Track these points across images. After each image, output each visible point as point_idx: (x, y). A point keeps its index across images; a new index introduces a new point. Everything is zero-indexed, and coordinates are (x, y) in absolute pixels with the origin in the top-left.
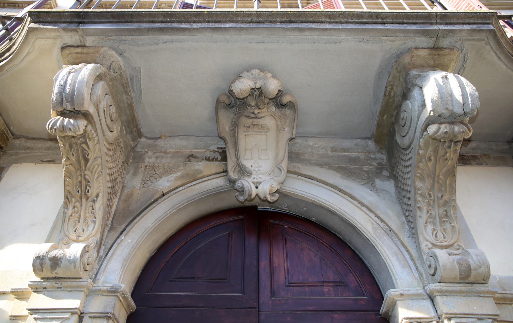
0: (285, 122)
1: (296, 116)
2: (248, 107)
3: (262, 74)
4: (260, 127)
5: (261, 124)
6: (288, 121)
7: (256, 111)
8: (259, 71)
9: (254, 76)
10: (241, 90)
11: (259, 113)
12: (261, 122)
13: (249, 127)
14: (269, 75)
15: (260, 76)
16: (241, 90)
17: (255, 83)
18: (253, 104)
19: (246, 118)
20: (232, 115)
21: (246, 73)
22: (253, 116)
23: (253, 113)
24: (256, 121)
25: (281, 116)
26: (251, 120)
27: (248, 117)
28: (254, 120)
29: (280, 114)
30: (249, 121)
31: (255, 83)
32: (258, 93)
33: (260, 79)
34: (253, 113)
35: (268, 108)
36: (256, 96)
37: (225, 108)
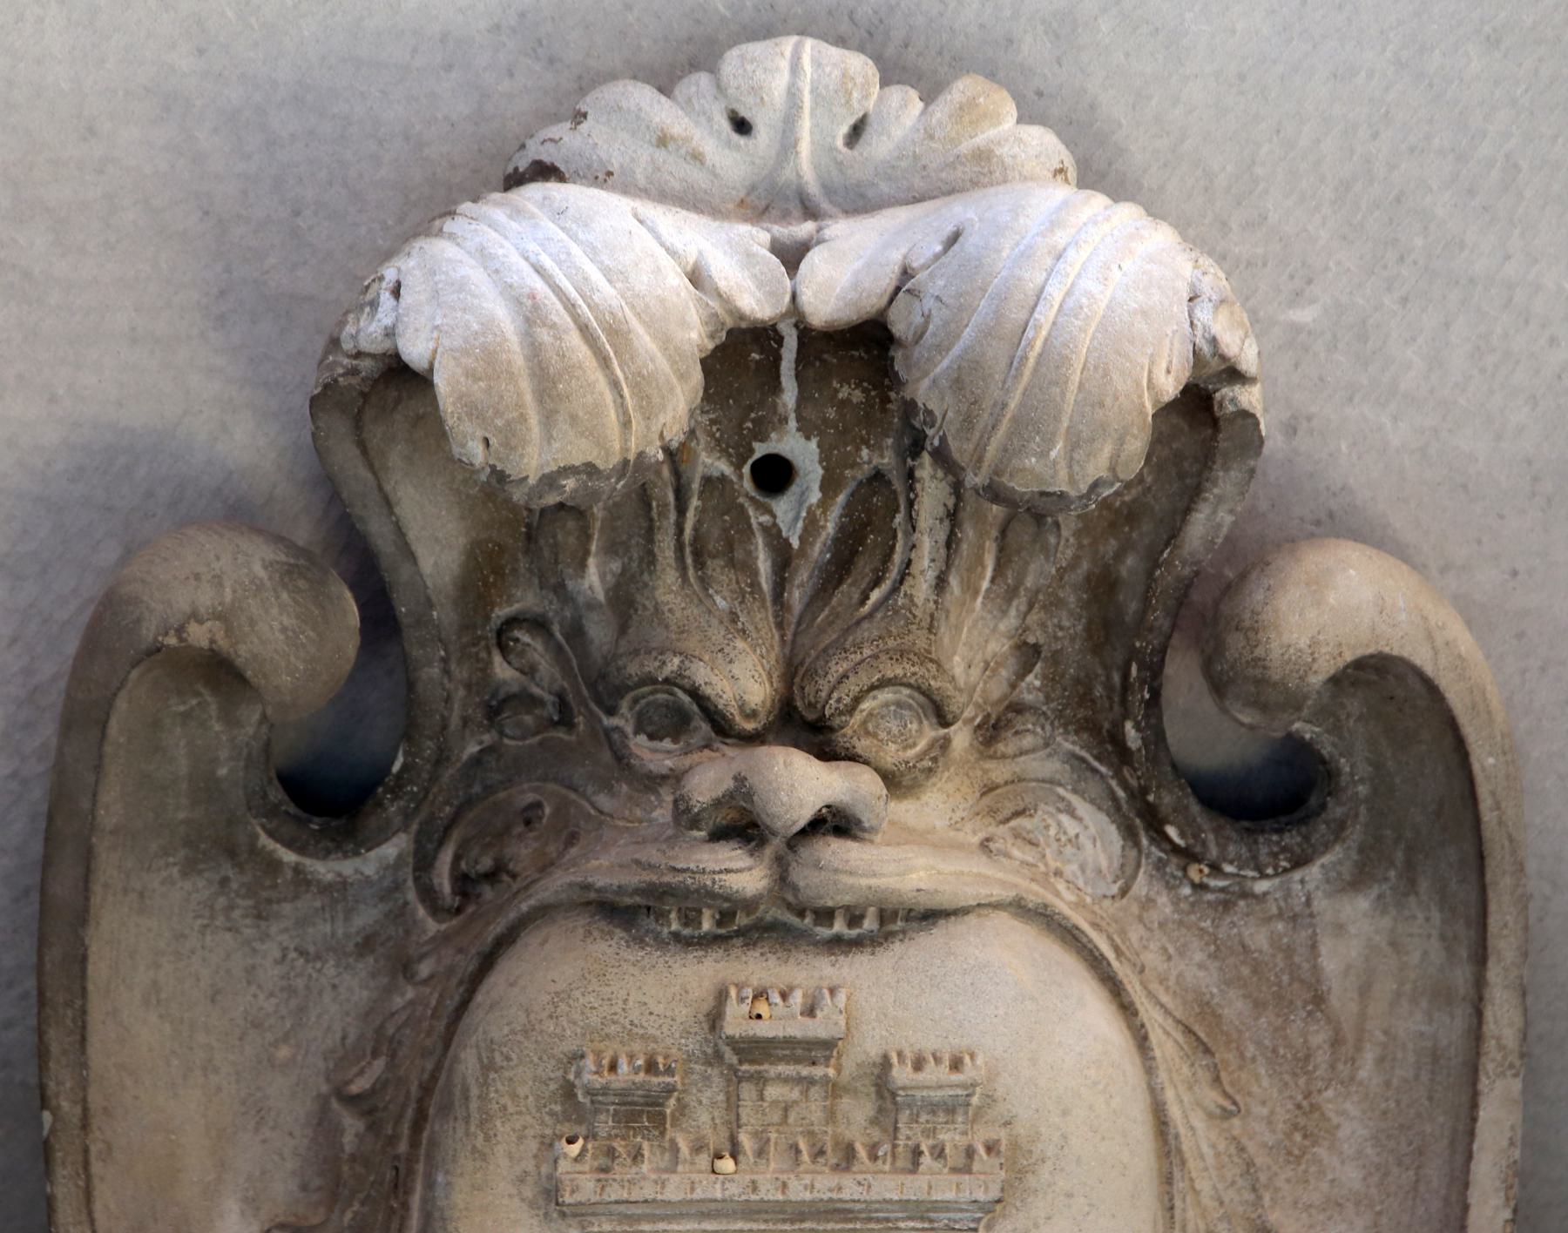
0: (1307, 1128)
1: (1502, 1018)
2: (653, 755)
3: (903, 114)
4: (857, 1115)
5: (868, 1044)
6: (1351, 1123)
7: (799, 783)
8: (860, 65)
9: (764, 135)
10: (531, 315)
11: (835, 823)
12: (879, 1003)
13: (647, 1111)
14: (1039, 145)
15: (878, 146)
16: (531, 315)
17: (791, 256)
18: (743, 680)
19: (608, 947)
20: (343, 997)
21: (642, 96)
22: (742, 873)
23: (742, 825)
24: (778, 991)
25: (1234, 1008)
26: (698, 974)
27: (628, 913)
28: (756, 967)
29: (1197, 969)
30: (652, 996)
31: (791, 256)
32: (835, 393)
33: (859, 202)
34: (742, 825)
35: (1004, 806)
36: (784, 559)
37: (214, 846)
